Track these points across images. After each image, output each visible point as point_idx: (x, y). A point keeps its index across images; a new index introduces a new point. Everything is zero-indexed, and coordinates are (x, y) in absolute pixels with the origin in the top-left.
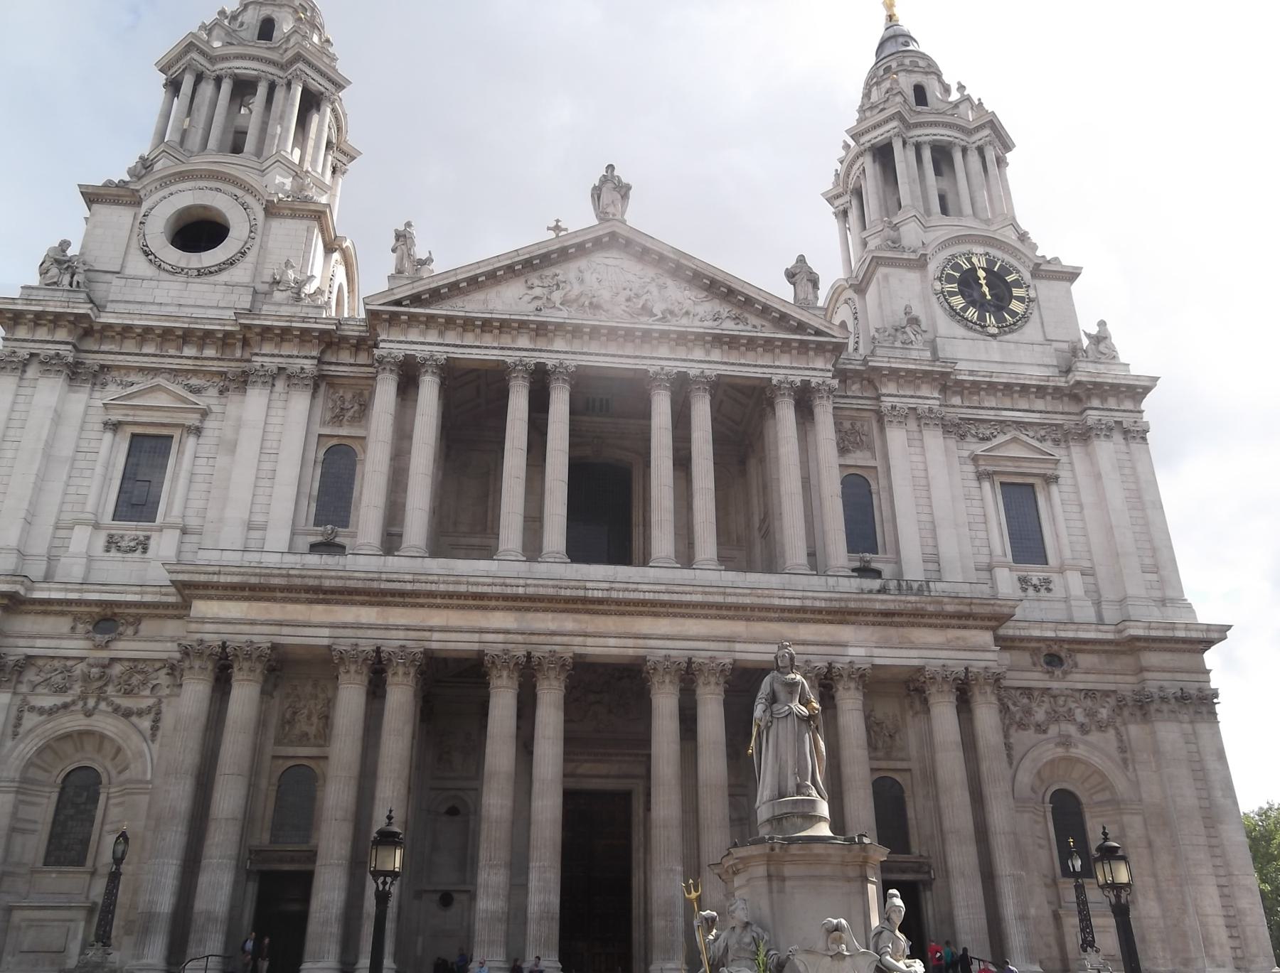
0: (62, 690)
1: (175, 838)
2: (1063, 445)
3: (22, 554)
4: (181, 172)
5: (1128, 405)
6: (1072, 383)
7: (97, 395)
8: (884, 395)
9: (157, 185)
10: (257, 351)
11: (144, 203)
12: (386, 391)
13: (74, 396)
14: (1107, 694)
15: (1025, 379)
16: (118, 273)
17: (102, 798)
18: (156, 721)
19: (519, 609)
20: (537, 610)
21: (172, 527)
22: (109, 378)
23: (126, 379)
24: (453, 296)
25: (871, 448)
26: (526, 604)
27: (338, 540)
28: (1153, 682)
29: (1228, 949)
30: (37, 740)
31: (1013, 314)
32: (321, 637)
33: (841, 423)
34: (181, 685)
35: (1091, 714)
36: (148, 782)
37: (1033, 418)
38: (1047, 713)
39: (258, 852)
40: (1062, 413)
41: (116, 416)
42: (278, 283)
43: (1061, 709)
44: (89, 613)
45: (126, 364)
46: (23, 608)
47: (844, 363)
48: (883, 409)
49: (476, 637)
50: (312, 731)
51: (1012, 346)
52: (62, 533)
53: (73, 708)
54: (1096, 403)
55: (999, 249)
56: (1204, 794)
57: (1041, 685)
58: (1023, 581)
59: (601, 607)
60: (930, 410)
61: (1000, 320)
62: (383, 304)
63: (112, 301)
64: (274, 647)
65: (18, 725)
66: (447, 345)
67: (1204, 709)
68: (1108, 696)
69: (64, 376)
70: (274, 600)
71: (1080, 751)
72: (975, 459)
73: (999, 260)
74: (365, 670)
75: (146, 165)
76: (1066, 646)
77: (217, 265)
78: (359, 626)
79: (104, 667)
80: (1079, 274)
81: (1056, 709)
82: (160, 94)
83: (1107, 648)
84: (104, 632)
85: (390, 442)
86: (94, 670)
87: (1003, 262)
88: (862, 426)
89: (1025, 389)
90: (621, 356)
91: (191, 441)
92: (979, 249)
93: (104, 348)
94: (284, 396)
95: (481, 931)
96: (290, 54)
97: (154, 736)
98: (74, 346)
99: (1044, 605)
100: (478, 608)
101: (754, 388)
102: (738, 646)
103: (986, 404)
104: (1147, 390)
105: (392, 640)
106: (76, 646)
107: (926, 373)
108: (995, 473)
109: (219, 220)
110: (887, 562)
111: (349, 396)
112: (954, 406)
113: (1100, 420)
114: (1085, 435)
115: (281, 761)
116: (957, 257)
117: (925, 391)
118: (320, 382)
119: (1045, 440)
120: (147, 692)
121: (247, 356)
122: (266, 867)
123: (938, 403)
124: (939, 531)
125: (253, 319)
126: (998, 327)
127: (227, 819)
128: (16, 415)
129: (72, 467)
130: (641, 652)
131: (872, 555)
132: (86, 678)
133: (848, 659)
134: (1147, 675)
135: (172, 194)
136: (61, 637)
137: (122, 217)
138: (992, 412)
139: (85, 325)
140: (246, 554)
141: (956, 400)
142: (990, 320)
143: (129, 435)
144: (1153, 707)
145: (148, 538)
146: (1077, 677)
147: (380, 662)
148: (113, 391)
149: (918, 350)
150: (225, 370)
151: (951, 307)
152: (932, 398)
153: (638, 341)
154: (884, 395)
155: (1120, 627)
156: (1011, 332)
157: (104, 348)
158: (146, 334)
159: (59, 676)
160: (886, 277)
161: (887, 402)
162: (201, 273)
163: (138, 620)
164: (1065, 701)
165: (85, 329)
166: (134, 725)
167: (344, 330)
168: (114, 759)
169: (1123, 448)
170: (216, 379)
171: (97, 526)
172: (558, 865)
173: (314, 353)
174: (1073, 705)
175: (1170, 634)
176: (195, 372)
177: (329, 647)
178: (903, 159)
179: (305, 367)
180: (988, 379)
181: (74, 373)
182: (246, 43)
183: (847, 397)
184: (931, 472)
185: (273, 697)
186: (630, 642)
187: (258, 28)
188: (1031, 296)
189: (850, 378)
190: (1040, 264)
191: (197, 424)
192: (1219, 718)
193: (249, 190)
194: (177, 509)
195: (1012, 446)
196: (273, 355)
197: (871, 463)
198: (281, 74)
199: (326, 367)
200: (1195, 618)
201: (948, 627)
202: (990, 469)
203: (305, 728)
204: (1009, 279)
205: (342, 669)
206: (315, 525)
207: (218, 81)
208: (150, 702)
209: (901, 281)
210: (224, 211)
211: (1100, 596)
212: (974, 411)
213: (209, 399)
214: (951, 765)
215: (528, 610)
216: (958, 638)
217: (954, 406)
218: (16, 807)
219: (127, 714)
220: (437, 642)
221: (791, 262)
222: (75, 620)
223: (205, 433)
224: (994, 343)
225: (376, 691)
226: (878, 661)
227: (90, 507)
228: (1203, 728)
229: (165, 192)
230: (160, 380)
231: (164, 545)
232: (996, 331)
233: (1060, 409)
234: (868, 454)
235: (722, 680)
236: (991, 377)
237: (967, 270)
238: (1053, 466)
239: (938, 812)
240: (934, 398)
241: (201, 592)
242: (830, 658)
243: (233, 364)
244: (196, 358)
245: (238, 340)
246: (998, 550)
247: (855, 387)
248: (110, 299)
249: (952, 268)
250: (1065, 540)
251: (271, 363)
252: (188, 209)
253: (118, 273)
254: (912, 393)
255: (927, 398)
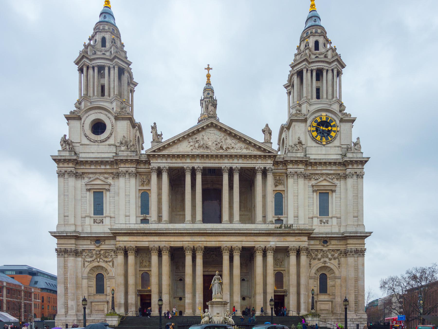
0: (91, 257)
1: (122, 289)
2: (339, 180)
3: (76, 225)
4: (90, 108)
5: (360, 167)
6: (344, 161)
7: (83, 181)
8: (288, 168)
9: (84, 112)
10: (120, 166)
11: (82, 119)
12: (154, 177)
13: (78, 182)
14: (338, 250)
15: (330, 160)
16: (80, 143)
17: (105, 280)
18: (113, 263)
19: (191, 236)
20: (195, 236)
21: (108, 217)
22: (84, 176)
23: (88, 176)
24: (168, 147)
25: (284, 185)
26: (192, 235)
27: (147, 218)
28: (349, 247)
29: (354, 308)
30: (89, 268)
31: (331, 137)
32: (146, 244)
33: (276, 177)
34: (117, 255)
35: (332, 255)
36: (114, 277)
37: (332, 172)
38: (321, 255)
39: (139, 291)
40: (340, 170)
41: (89, 187)
42: (122, 144)
43: (325, 254)
44: (94, 239)
45: (88, 172)
46: (79, 238)
47: (277, 159)
48: (287, 173)
49: (181, 243)
50: (147, 265)
51: (329, 148)
52: (83, 219)
53: (95, 261)
54: (350, 166)
55: (331, 113)
56: (357, 274)
57: (321, 248)
58: (321, 221)
59: (210, 235)
60: (301, 172)
61: (327, 139)
62: (150, 152)
63: (81, 153)
64: (136, 247)
65: (84, 265)
66: (168, 163)
67: (361, 254)
68: (338, 251)
69: (74, 177)
70: (135, 236)
71: (328, 265)
72: (313, 186)
73: (330, 117)
74: (157, 252)
75: (79, 102)
76: (329, 238)
77: (104, 139)
78: (155, 241)
79: (99, 251)
80: (355, 120)
81: (324, 254)
82: (77, 73)
83: (340, 238)
84: (98, 243)
85: (157, 192)
86: (98, 252)
87: (331, 118)
88: (282, 178)
89: (330, 163)
90: (214, 163)
91: (108, 193)
92: (324, 114)
93: (82, 167)
94: (128, 179)
95: (187, 306)
96: (113, 56)
97: (113, 267)
98: (75, 168)
99: (325, 227)
100: (181, 236)
101: (251, 169)
102: (243, 243)
103: (318, 169)
104: (366, 161)
105: (162, 245)
106: (92, 247)
107: (301, 161)
108: (318, 190)
109: (103, 122)
110: (285, 217)
111: (145, 177)
112: (309, 170)
113: (350, 172)
114: (345, 177)
115: (141, 272)
116: (317, 118)
117: (300, 166)
118: (137, 174)
119: (334, 179)
120: (110, 257)
121: (117, 168)
122: (141, 294)
123: (303, 169)
124: (299, 209)
125: (118, 157)
126: (326, 142)
127: (132, 285)
128: (65, 189)
129: (81, 202)
130: (220, 245)
131: (281, 216)
132: (96, 254)
133: (270, 245)
134: (348, 245)
135: (89, 115)
136: (89, 245)
137: (76, 124)
138: (320, 171)
139: (76, 161)
140: (126, 225)
141: (310, 168)
142: (324, 139)
143: (93, 192)
144: (349, 253)
145: (103, 219)
146: (330, 246)
147: (160, 249)
148: (86, 180)
149: (300, 152)
150: (113, 172)
151: (312, 136)
152: (302, 168)
153: (219, 158)
154: (288, 168)
155: (343, 233)
156: (330, 143)
157: (82, 167)
158: (91, 163)
159: (90, 254)
160: (294, 126)
161: (289, 170)
162: (102, 141)
163: (104, 240)
164: (326, 252)
165: (77, 162)
166: (108, 265)
167: (141, 158)
168: (105, 271)
169: (356, 181)
170: (111, 175)
171: (91, 217)
172: (202, 293)
173: (135, 166)
174: (328, 253)
175: (356, 235)
176: (105, 173)
177: (148, 246)
178: (306, 76)
179: (133, 170)
180: (319, 161)
181: (76, 175)
182: (98, 50)
183: (278, 169)
184: (299, 191)
185: (137, 257)
186: (218, 243)
187: (101, 42)
188: (338, 130)
189: (279, 163)
190: (343, 118)
191: (108, 188)
192: (365, 256)
193: (109, 112)
194: (108, 212)
195: (325, 181)
196: (124, 167)
197: (283, 189)
198: (111, 63)
199: (138, 170)
200: (365, 230)
201: (296, 236)
202: (316, 189)
203: (145, 264)
204: (332, 124)
205: (152, 252)
206: (141, 214)
207: (93, 68)
208: (110, 259)
209: (299, 127)
210: (104, 120)
211: (341, 224)
212: (314, 171)
213: (110, 181)
214: (293, 270)
215: (193, 236)
216: (298, 239)
217: (309, 170)
218: (88, 282)
219: (107, 262)
220: (173, 244)
221: (264, 127)
222: (91, 241)
223: (111, 190)
224: (324, 148)
225: (160, 255)
226: (277, 245)
227: (88, 212)
228: (360, 259)
229: (87, 115)
230: (97, 176)
231: (107, 221)
232: (324, 143)
233: (340, 169)
234: (283, 186)
235: (239, 252)
236: (320, 160)
237: (319, 122)
238: (335, 187)
239: (289, 280)
240: (303, 168)
241: (118, 235)
242: (265, 245)
243: (114, 170)
244: (105, 169)
245: (115, 163)
246: (315, 213)
247: (281, 166)
248: (80, 152)
249: (315, 122)
250: (334, 209)
251: (124, 170)
252: (94, 120)
253: (80, 143)
254: (297, 167)
255: (301, 168)
